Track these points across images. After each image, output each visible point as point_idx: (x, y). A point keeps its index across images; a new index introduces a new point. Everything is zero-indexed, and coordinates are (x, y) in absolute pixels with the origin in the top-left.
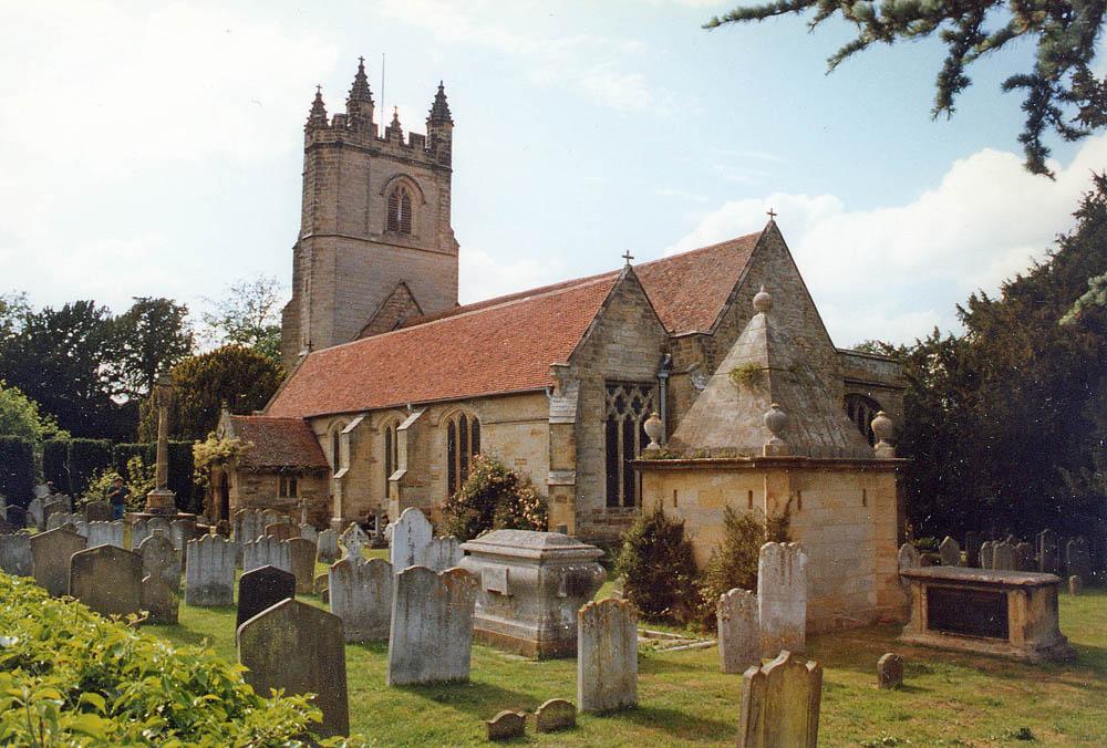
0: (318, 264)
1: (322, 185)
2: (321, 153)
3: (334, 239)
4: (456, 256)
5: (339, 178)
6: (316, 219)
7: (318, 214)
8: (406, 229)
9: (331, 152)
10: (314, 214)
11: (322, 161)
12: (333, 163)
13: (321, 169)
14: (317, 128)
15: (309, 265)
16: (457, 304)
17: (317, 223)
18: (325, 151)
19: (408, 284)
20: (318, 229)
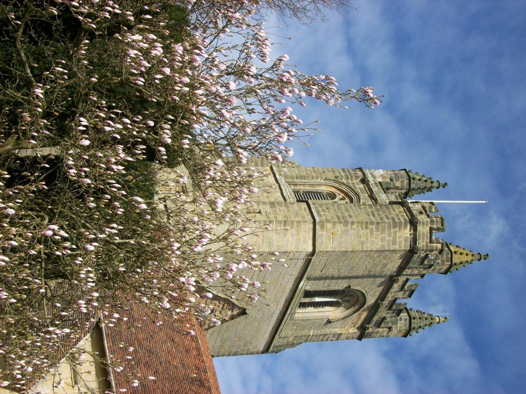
0: (281, 228)
1: (372, 230)
2: (405, 227)
3: (310, 249)
4: (266, 350)
5: (377, 251)
6: (334, 223)
7: (340, 227)
8: (303, 305)
9: (406, 241)
10: (340, 222)
11: (397, 229)
12: (394, 243)
13: (389, 228)
14: (432, 221)
15: (280, 218)
16: (213, 356)
17: (329, 225)
18: (407, 232)
19: (242, 317)
20: (322, 227)
